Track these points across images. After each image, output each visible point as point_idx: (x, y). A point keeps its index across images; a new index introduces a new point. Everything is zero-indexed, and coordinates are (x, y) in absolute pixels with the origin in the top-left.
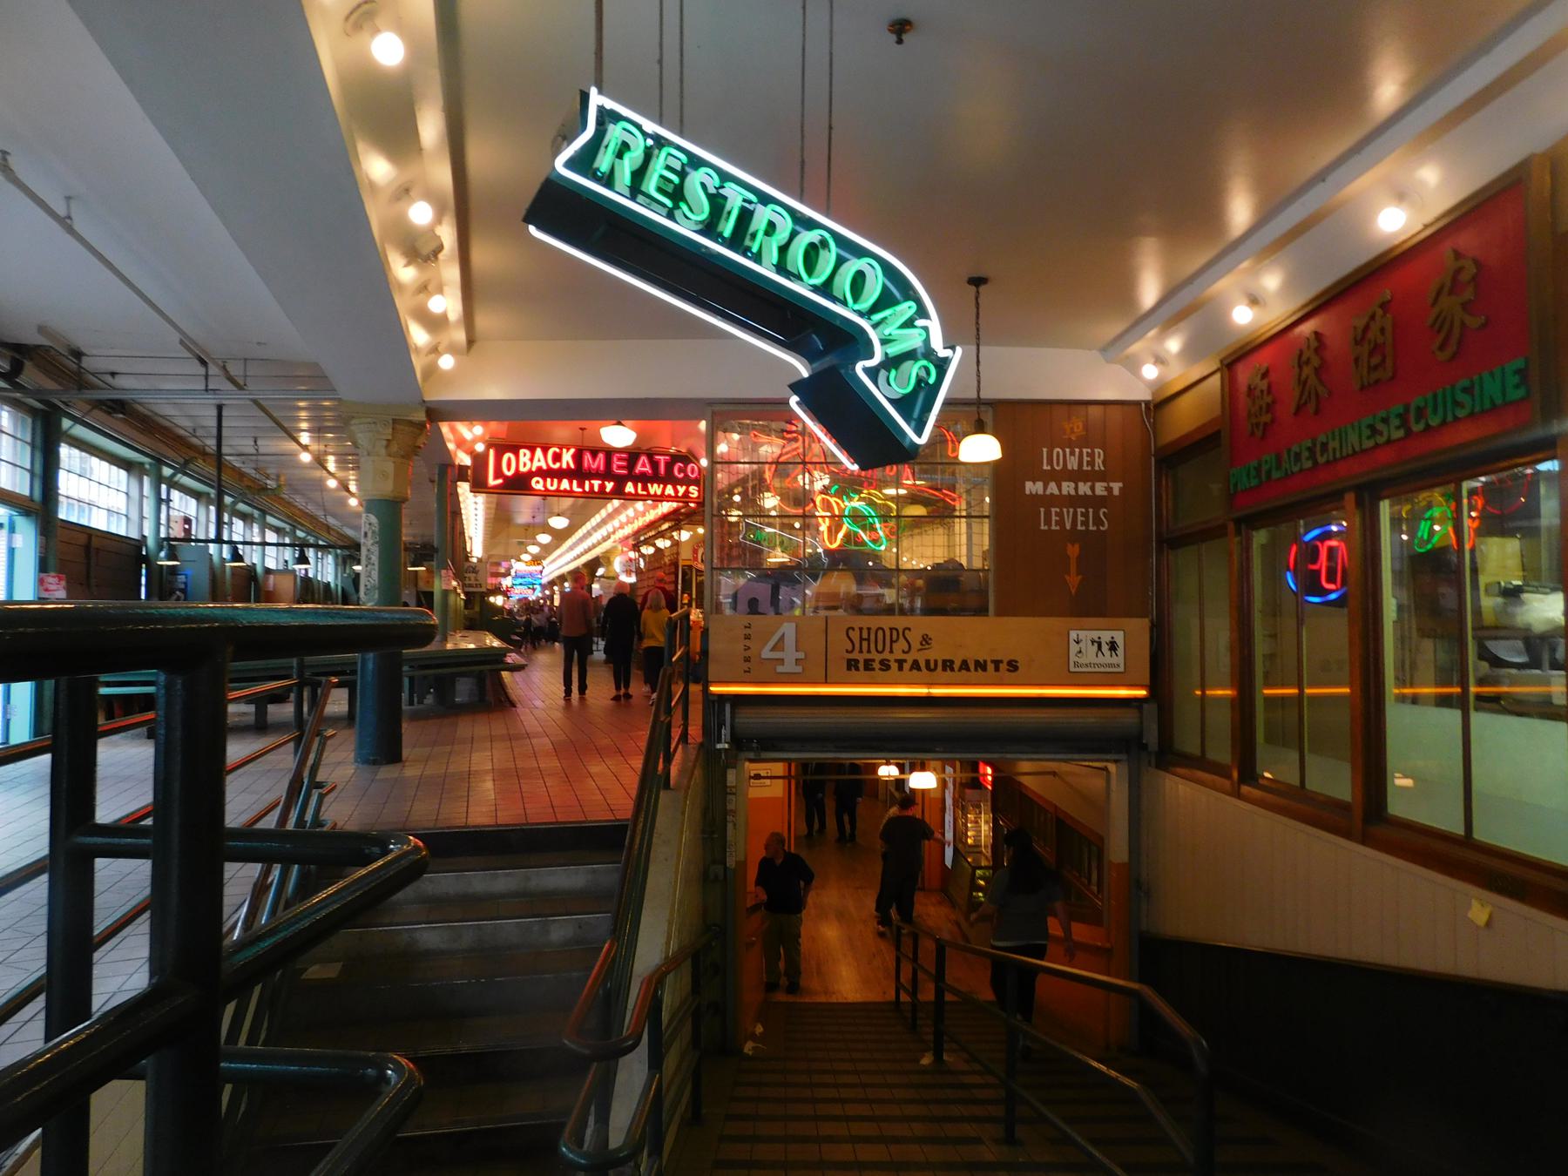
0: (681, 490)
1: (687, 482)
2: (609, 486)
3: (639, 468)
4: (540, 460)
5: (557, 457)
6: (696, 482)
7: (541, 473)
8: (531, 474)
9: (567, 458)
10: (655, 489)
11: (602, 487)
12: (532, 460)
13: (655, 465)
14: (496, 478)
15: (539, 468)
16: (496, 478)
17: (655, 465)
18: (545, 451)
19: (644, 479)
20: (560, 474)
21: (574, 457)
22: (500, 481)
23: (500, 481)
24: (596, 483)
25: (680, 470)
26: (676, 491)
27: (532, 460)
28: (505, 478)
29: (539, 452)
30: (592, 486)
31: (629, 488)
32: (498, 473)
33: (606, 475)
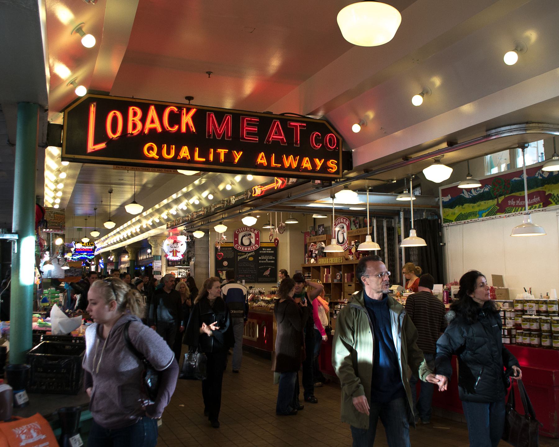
0: (319, 163)
1: (326, 155)
2: (238, 156)
3: (274, 136)
4: (153, 122)
5: (175, 119)
6: (334, 155)
7: (153, 136)
8: (143, 138)
9: (187, 119)
10: (290, 161)
11: (229, 156)
12: (143, 120)
13: (289, 132)
14: (95, 143)
15: (153, 131)
16: (95, 143)
17: (289, 132)
18: (160, 111)
19: (277, 150)
20: (178, 140)
21: (193, 118)
22: (102, 146)
23: (102, 146)
24: (222, 152)
25: (317, 141)
26: (314, 165)
27: (143, 120)
28: (110, 142)
29: (152, 113)
30: (217, 155)
31: (261, 159)
32: (100, 136)
33: (233, 144)
